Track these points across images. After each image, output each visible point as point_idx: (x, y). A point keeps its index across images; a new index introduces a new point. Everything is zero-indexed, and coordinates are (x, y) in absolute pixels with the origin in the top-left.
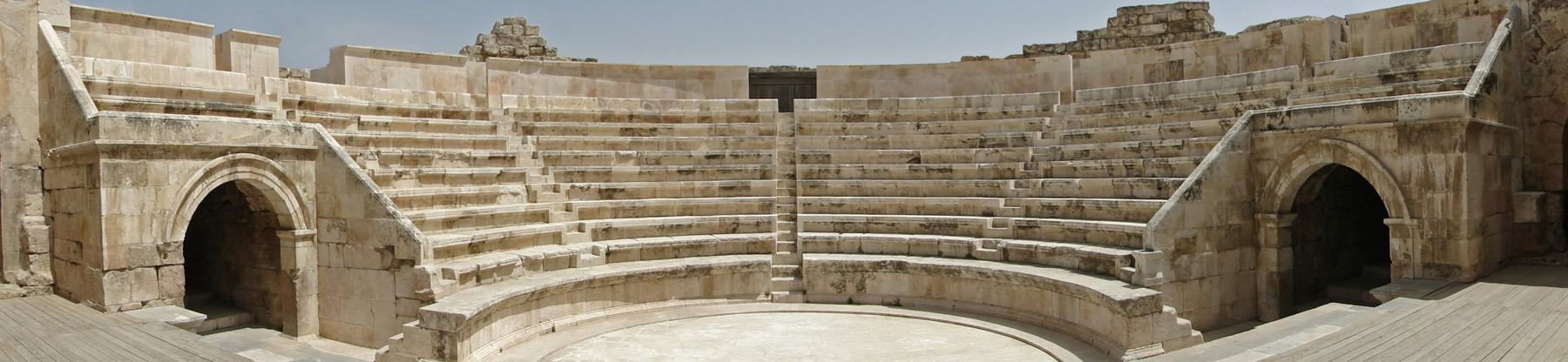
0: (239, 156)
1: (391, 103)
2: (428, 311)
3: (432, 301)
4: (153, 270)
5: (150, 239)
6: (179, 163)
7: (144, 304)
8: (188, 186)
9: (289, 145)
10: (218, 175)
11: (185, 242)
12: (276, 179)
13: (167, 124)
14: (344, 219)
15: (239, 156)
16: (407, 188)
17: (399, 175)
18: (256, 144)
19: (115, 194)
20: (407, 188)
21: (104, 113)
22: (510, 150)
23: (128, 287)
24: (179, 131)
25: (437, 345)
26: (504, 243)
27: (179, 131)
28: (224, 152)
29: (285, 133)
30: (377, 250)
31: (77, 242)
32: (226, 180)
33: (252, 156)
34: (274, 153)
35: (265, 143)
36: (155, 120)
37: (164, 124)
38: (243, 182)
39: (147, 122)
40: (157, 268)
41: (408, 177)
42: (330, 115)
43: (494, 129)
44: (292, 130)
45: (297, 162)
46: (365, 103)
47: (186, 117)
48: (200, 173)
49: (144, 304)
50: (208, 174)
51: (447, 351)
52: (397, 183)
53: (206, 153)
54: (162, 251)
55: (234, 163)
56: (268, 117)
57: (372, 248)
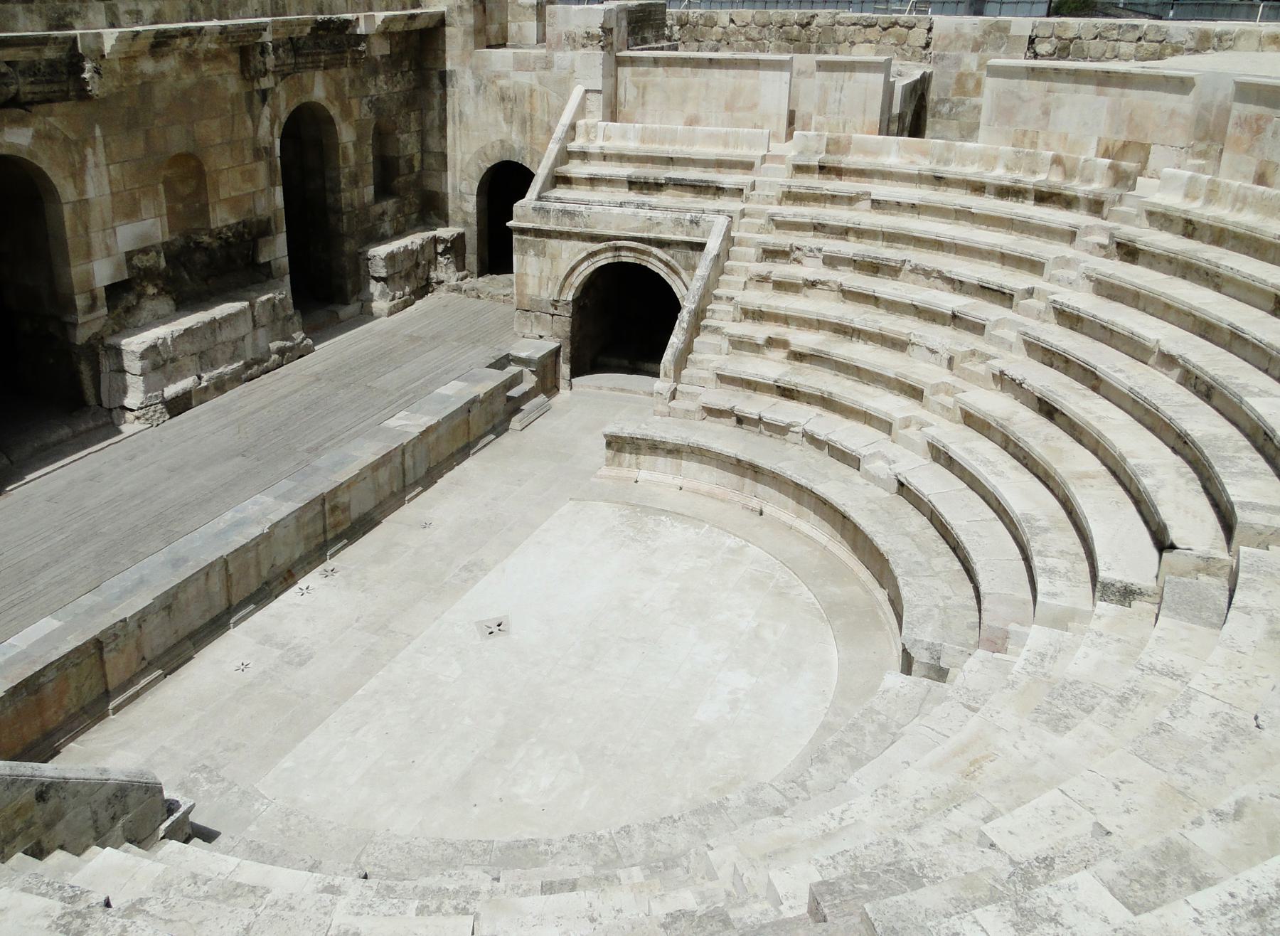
0: (620, 243)
5: (549, 293)
6: (571, 243)
7: (541, 337)
8: (573, 263)
10: (603, 256)
12: (662, 266)
15: (620, 243)
19: (523, 259)
23: (530, 323)
24: (572, 219)
27: (572, 219)
28: (609, 238)
29: (678, 225)
32: (610, 261)
33: (634, 244)
39: (548, 212)
41: (825, 287)
44: (688, 224)
45: (691, 252)
48: (584, 254)
49: (541, 337)
54: (555, 304)
55: (618, 249)
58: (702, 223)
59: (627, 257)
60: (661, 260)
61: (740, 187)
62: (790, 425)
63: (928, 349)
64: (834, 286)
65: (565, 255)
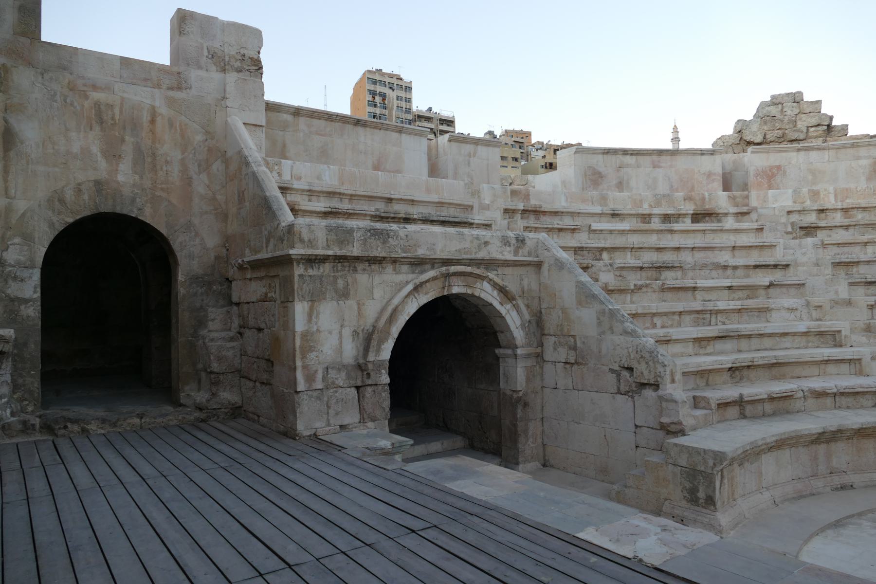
0: (453, 269)
1: (628, 208)
2: (676, 445)
3: (682, 432)
4: (353, 391)
9: (510, 257)
11: (391, 361)
12: (495, 293)
13: (372, 235)
14: (574, 337)
15: (453, 269)
16: (649, 302)
17: (638, 288)
18: (473, 256)
20: (649, 302)
21: (301, 221)
22: (778, 256)
25: (688, 485)
26: (775, 368)
28: (434, 263)
30: (612, 371)
31: (268, 360)
33: (468, 269)
34: (491, 264)
35: (481, 255)
36: (359, 229)
37: (369, 234)
38: (458, 296)
40: (358, 388)
42: (556, 222)
43: (760, 230)
44: (513, 241)
46: (598, 209)
47: (394, 227)
48: (410, 287)
51: (701, 495)
52: (636, 297)
53: (419, 263)
55: (447, 276)
56: (487, 226)
57: (606, 369)
61: (490, 222)
63: (788, 309)
64: (655, 287)
65: (377, 294)
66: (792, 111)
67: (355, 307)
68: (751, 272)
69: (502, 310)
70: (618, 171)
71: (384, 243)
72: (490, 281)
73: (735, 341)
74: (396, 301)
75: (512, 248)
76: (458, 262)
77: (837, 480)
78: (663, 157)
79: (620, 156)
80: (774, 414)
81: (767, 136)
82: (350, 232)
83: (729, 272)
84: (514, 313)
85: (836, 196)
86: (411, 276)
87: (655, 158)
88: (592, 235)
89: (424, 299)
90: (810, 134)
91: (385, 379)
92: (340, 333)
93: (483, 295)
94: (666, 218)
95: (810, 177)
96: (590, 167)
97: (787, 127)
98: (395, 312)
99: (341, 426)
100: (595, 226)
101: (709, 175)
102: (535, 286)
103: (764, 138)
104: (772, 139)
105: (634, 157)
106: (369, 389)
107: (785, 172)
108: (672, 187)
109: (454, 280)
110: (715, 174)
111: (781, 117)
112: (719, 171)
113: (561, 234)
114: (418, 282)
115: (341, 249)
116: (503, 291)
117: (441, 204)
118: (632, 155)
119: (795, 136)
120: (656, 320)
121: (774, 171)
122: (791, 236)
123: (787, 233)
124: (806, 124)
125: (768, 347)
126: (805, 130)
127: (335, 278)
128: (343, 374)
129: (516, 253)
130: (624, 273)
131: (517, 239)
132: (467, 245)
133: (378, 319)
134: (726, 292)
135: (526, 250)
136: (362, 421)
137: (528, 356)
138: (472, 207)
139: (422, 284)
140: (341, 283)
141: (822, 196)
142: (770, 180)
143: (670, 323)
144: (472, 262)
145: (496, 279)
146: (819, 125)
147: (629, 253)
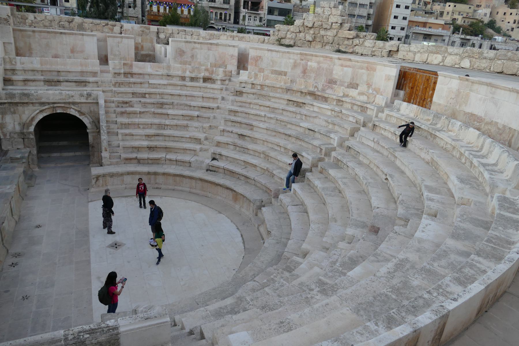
0: (55, 105)
12: (77, 112)
15: (55, 105)
28: (49, 103)
33: (63, 105)
34: (74, 103)
36: (17, 94)
48: (38, 111)
50: (41, 111)
55: (54, 107)
58: (92, 94)
59: (59, 111)
60: (76, 110)
62: (161, 158)
65: (27, 112)
66: (328, 12)
67: (19, 116)
68: (201, 109)
69: (81, 118)
70: (192, 50)
71: (28, 97)
72: (73, 109)
73: (164, 137)
74: (32, 115)
75: (85, 98)
76: (59, 103)
77: (156, 186)
78: (213, 46)
79: (193, 44)
80: (152, 164)
81: (315, 24)
82: (14, 95)
83: (192, 108)
84: (86, 119)
85: (263, 78)
86: (39, 107)
87: (209, 46)
88: (150, 85)
89: (45, 114)
90: (333, 27)
91: (32, 136)
92: (14, 123)
93: (71, 113)
94: (192, 79)
95: (271, 64)
96: (179, 48)
97: (324, 21)
98: (33, 119)
99: (18, 149)
100: (151, 81)
101: (232, 56)
102: (96, 110)
103: (313, 25)
104: (316, 26)
105: (200, 45)
106: (26, 139)
107: (262, 60)
108: (216, 59)
109: (57, 109)
110: (234, 56)
111: (322, 15)
112: (236, 54)
113: (135, 84)
114: (41, 109)
115: (11, 100)
116: (79, 111)
117: (82, 73)
118: (198, 44)
119: (325, 26)
120: (140, 126)
121: (258, 58)
122: (232, 94)
123: (231, 93)
124: (332, 21)
125: (176, 140)
126: (330, 24)
127: (10, 108)
128: (16, 135)
129: (87, 99)
130: (146, 105)
131: (87, 94)
132: (64, 97)
133: (27, 120)
134: (182, 116)
135: (92, 98)
136: (24, 147)
137: (93, 132)
138: (97, 72)
139: (43, 110)
140: (12, 110)
141: (258, 77)
142: (256, 62)
143: (147, 127)
144: (64, 103)
145: (75, 108)
146: (337, 23)
147: (158, 95)
